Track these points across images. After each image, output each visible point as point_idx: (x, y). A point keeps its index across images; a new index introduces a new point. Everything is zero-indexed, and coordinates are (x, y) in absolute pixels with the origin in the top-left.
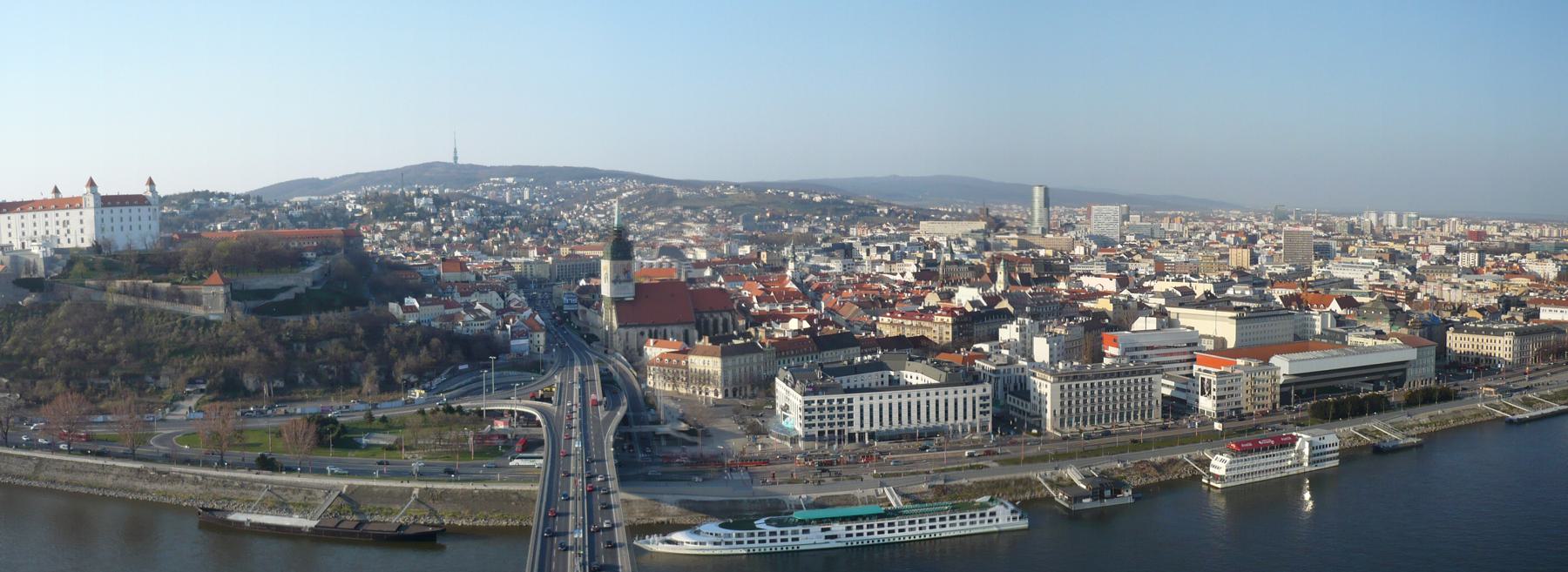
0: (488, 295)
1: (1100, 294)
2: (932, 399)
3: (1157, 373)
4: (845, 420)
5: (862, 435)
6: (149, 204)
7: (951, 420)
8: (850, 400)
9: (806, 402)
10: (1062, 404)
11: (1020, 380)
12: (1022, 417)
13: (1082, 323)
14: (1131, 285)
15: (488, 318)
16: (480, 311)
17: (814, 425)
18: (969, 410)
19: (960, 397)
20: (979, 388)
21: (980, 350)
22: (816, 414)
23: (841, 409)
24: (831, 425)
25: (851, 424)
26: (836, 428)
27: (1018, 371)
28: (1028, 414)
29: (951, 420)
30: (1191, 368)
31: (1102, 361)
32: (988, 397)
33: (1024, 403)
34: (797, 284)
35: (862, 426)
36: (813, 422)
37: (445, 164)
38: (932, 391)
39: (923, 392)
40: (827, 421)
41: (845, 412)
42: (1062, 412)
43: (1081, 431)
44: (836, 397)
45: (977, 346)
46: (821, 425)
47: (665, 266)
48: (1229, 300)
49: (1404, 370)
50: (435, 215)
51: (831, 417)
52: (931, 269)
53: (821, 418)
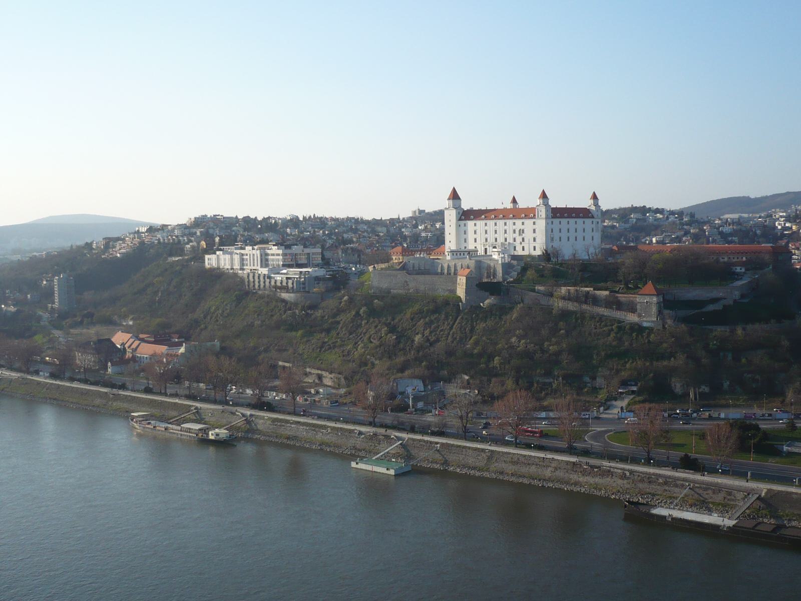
6: (593, 217)
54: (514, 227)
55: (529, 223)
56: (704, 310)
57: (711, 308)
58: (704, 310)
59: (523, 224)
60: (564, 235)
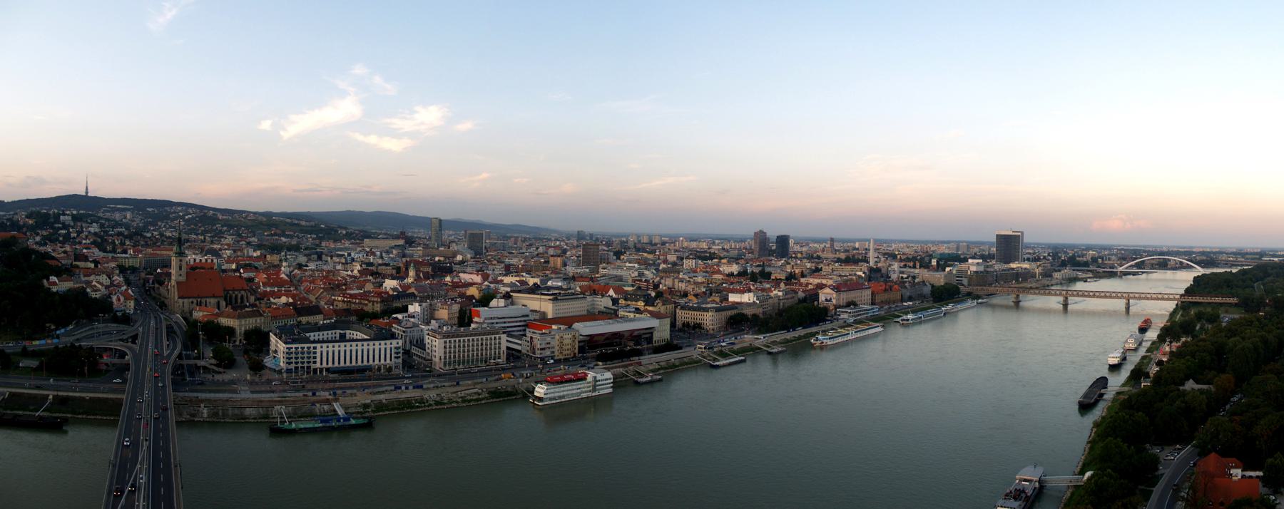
1: (471, 284)
2: (365, 348)
3: (504, 333)
4: (312, 360)
5: (321, 370)
7: (377, 362)
8: (315, 348)
9: (287, 348)
10: (445, 353)
12: (421, 360)
13: (459, 303)
14: (490, 279)
15: (100, 290)
16: (95, 286)
17: (292, 363)
18: (388, 356)
19: (383, 347)
20: (394, 342)
21: (396, 318)
22: (294, 356)
23: (309, 353)
24: (303, 363)
25: (315, 362)
26: (306, 365)
28: (424, 358)
29: (377, 362)
30: (525, 330)
31: (470, 326)
32: (400, 348)
34: (287, 275)
35: (321, 364)
36: (291, 361)
38: (365, 343)
39: (360, 343)
40: (300, 360)
41: (312, 355)
42: (445, 357)
43: (456, 369)
44: (306, 346)
45: (395, 316)
46: (297, 363)
48: (549, 288)
49: (652, 333)
51: (303, 358)
52: (369, 268)
53: (297, 358)
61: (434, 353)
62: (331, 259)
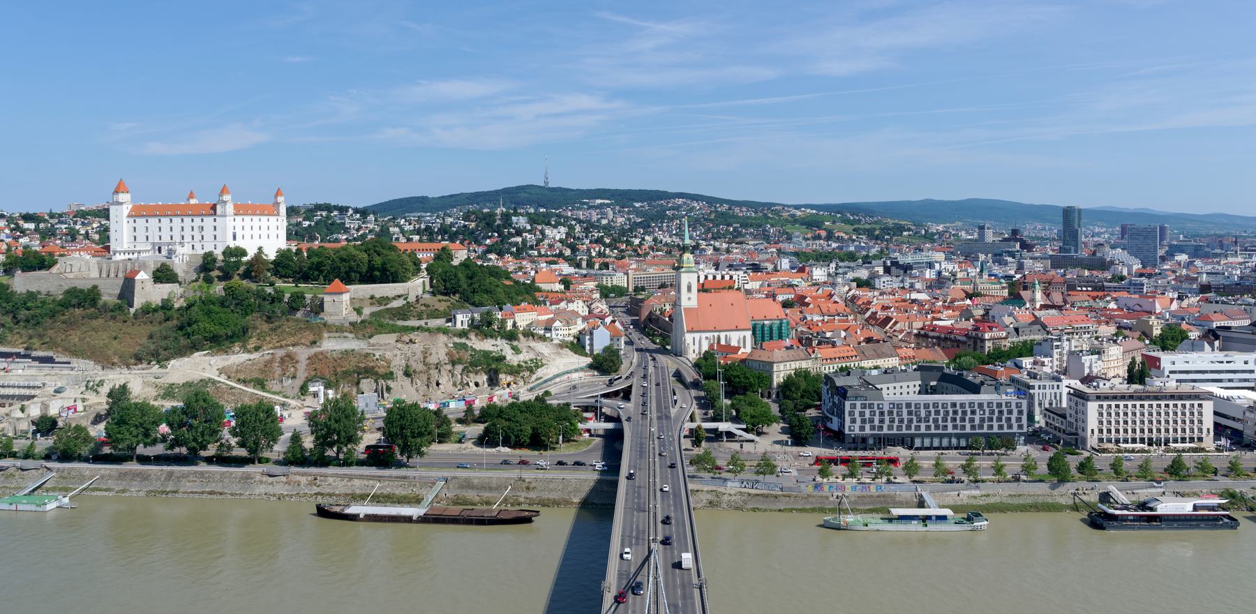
0: (575, 303)
10: (1101, 423)
11: (1056, 397)
27: (1053, 388)
28: (1064, 431)
33: (1060, 419)
37: (539, 187)
42: (1101, 431)
47: (727, 278)
50: (529, 232)
54: (193, 224)
55: (209, 221)
56: (387, 307)
57: (396, 304)
58: (388, 306)
59: (202, 220)
60: (247, 232)
61: (1080, 423)
62: (905, 272)
